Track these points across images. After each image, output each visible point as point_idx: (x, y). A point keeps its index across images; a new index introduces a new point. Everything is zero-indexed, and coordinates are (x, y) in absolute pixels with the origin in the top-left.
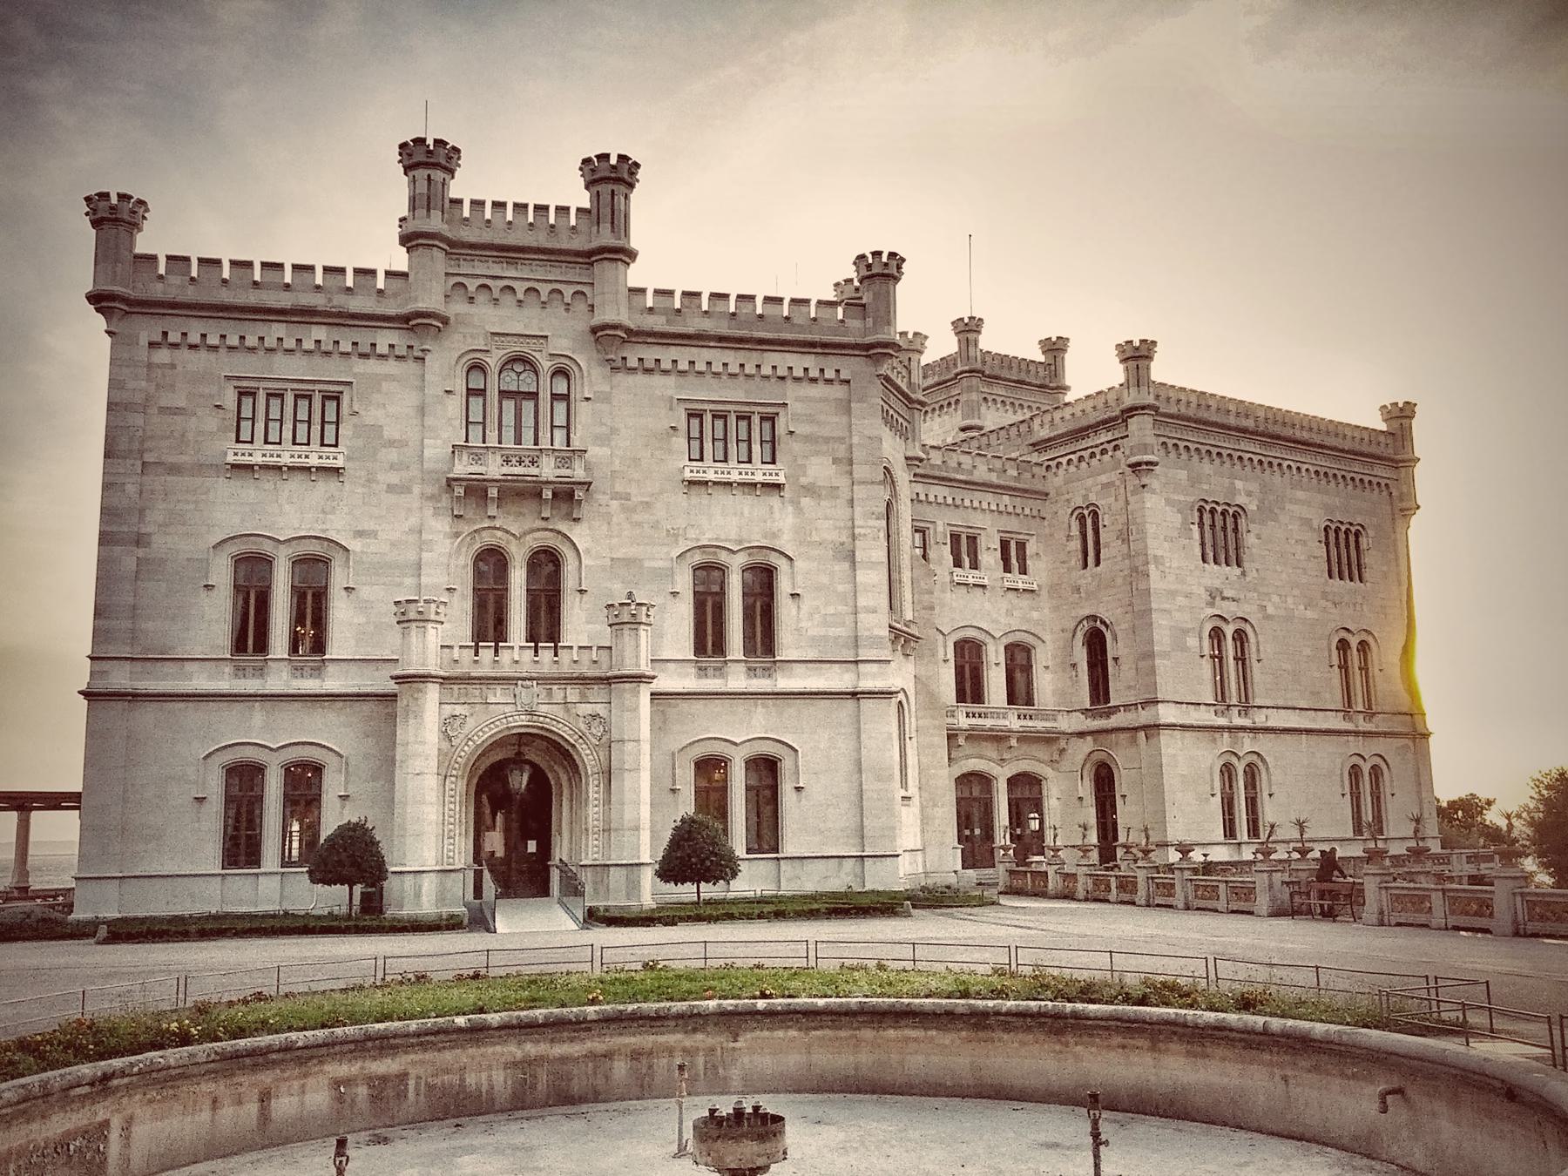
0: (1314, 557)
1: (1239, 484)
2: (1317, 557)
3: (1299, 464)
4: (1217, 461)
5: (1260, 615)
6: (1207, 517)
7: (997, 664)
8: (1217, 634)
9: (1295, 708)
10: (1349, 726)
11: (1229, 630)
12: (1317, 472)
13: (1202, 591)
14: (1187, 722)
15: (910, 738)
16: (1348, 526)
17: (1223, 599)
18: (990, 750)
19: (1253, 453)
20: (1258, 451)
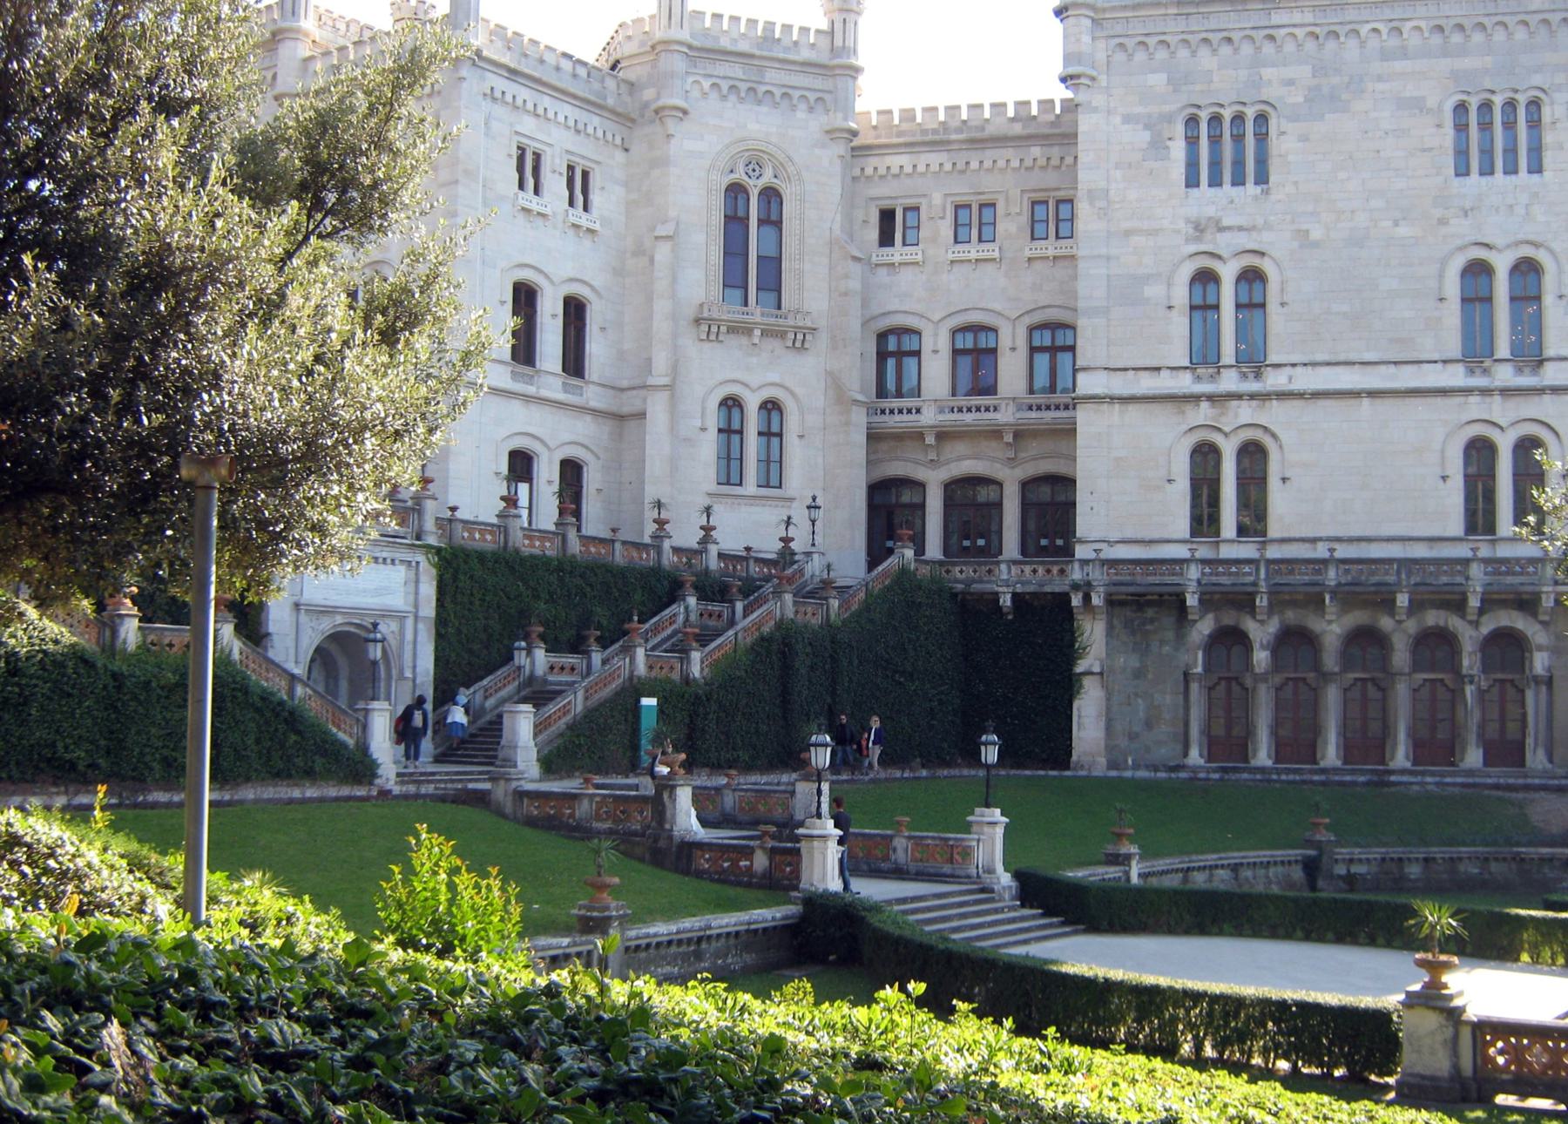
0: (1424, 150)
1: (1267, 73)
2: (1431, 149)
3: (1394, 24)
4: (1226, 50)
5: (1295, 244)
6: (1204, 127)
7: (1013, 349)
8: (1205, 278)
9: (1354, 363)
10: (1478, 381)
11: (1228, 273)
12: (1440, 29)
13: (1181, 225)
14: (1126, 392)
15: (801, 437)
16: (1511, 95)
17: (1222, 229)
18: (992, 447)
19: (1294, 26)
20: (1308, 17)
